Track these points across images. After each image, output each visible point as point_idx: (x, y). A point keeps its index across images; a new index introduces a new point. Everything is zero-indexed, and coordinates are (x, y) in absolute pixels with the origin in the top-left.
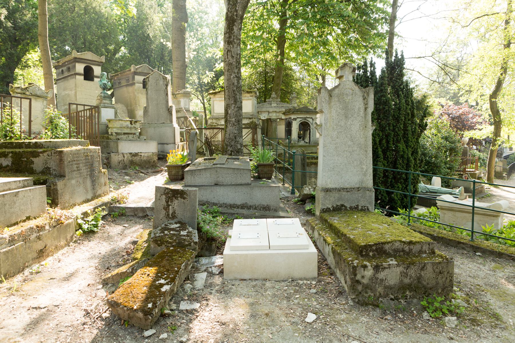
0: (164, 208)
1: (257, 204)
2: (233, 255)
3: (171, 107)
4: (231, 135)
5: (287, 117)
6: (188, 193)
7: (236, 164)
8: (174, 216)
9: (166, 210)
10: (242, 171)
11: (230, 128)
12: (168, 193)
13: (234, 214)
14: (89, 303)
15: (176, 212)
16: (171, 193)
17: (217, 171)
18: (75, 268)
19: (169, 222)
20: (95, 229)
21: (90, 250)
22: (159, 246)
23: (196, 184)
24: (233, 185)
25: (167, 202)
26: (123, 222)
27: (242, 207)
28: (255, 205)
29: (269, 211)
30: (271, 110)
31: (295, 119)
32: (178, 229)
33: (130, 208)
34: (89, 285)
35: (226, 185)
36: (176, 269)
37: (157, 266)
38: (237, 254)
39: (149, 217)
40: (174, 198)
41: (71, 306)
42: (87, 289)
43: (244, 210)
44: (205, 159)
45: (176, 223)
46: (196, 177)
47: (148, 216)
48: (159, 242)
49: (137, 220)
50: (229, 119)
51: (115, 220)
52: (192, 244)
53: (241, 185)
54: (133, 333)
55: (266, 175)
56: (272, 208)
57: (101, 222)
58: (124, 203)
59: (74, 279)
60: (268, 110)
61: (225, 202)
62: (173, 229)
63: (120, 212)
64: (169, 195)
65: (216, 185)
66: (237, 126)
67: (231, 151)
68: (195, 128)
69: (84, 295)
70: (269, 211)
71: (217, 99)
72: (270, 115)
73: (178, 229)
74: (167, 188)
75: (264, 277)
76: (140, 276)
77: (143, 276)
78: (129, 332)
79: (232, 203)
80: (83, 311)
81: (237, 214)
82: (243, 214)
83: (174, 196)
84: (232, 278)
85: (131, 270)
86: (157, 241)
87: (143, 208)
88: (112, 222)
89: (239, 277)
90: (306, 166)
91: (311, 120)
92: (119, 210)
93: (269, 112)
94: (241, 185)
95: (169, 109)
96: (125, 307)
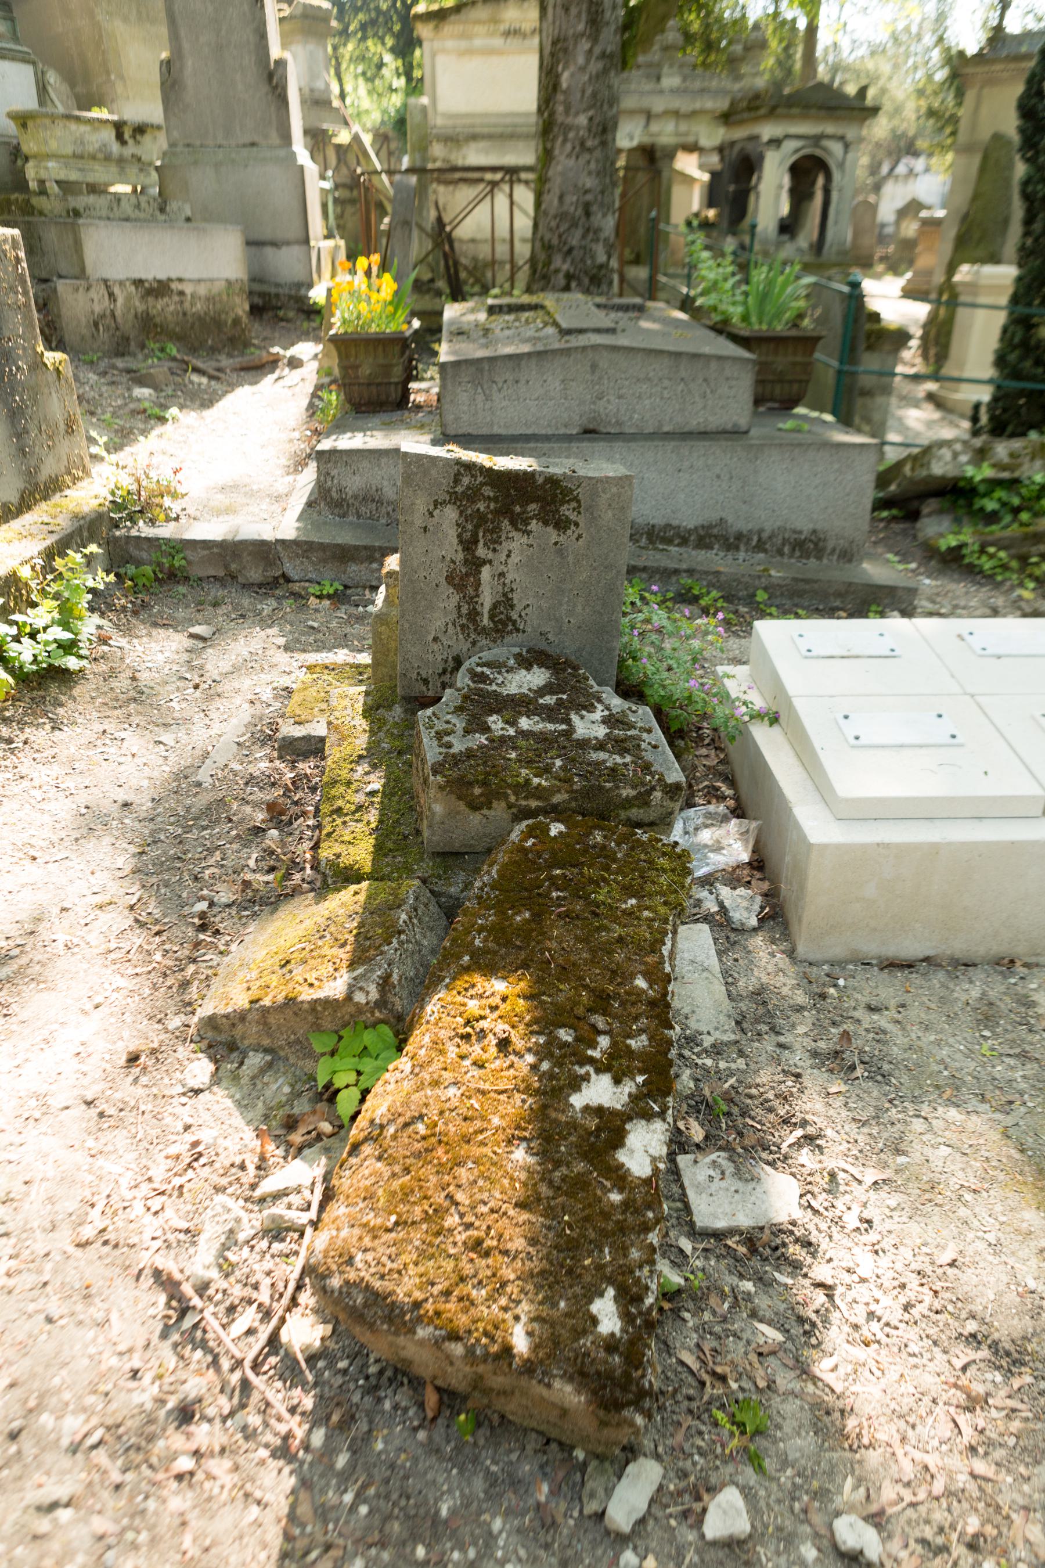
0: (450, 579)
1: (768, 527)
2: (864, 847)
3: (281, 63)
4: (571, 199)
5: (739, 133)
6: (581, 493)
7: (648, 331)
8: (503, 623)
9: (460, 588)
10: (714, 365)
11: (564, 162)
12: (472, 495)
13: (676, 572)
14: (174, 1217)
15: (516, 597)
16: (487, 491)
17: (594, 367)
18: (25, 905)
19: (486, 656)
20: (72, 663)
21: (70, 783)
22: (474, 807)
23: (496, 430)
24: (668, 436)
25: (468, 545)
26: (181, 614)
27: (701, 539)
28: (760, 531)
29: (819, 558)
30: (659, 105)
31: (776, 143)
32: (549, 700)
33: (205, 544)
34: (133, 1059)
35: (632, 437)
36: (641, 983)
37: (525, 965)
38: (887, 846)
39: (296, 587)
40: (506, 524)
41: (63, 1240)
42: (127, 1091)
43: (710, 554)
44: (492, 310)
45: (526, 662)
46: (496, 396)
47: (288, 580)
48: (477, 791)
49: (246, 602)
50: (560, 118)
51: (144, 605)
52: (658, 794)
53: (704, 435)
54: (515, 1483)
55: (777, 389)
56: (830, 545)
57: (89, 625)
58: (168, 519)
59: (89, 1248)
60: (646, 102)
61: (675, 523)
62: (522, 704)
63: (159, 564)
64: (481, 506)
65: (589, 432)
66: (598, 153)
67: (569, 277)
68: (379, 167)
69: (120, 1139)
70: (819, 558)
71: (450, 44)
72: (654, 127)
73: (549, 700)
74: (470, 467)
75: (997, 948)
76: (452, 1051)
77: (476, 1050)
78: (492, 1481)
79: (658, 520)
80: (147, 1281)
81: (690, 572)
82: (718, 573)
83: (505, 511)
84: (838, 951)
85: (374, 994)
86: (470, 784)
87: (263, 543)
88: (135, 613)
89: (872, 948)
90: (862, 345)
91: (836, 148)
92: (154, 556)
93: (649, 116)
94: (704, 435)
95: (270, 76)
96: (454, 1336)
